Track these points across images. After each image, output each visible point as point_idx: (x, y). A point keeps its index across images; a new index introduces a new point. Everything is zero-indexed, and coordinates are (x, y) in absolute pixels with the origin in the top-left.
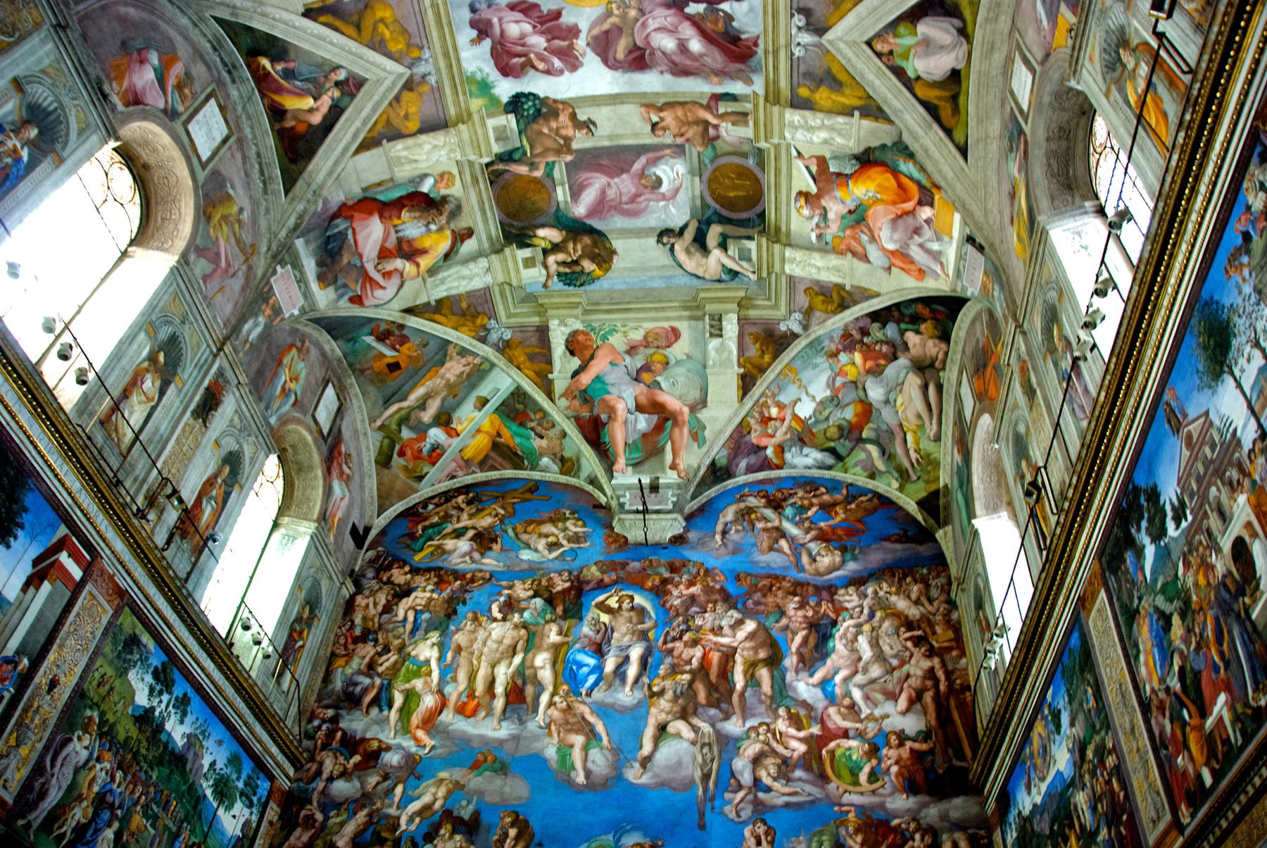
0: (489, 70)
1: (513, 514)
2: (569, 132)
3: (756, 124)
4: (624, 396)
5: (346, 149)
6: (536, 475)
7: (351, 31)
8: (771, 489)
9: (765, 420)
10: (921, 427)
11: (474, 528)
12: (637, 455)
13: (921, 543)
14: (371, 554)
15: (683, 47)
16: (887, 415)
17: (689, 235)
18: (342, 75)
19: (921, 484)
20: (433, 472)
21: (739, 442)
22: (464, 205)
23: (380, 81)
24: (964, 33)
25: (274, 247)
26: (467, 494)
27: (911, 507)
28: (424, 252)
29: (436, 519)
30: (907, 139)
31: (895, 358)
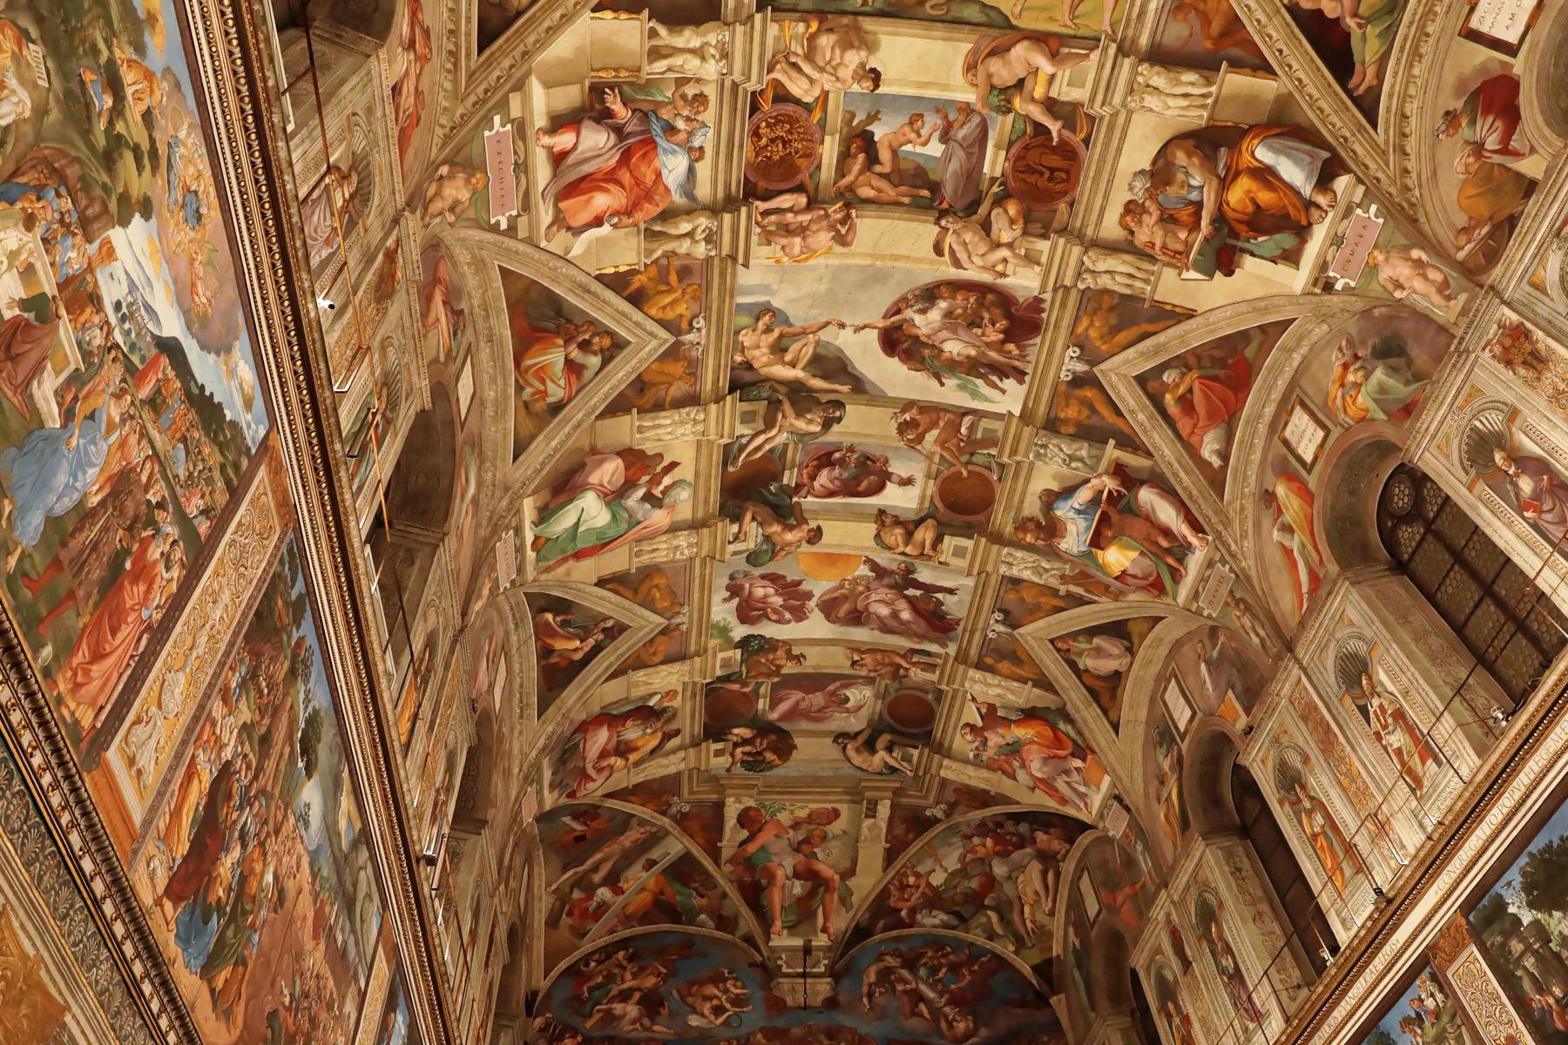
0: (732, 620)
1: (673, 973)
2: (783, 662)
3: (942, 674)
4: (785, 864)
5: (597, 679)
6: (692, 929)
7: (629, 594)
8: (903, 948)
9: (903, 887)
10: (1037, 902)
11: (639, 989)
12: (792, 918)
13: (1038, 1008)
14: (539, 1021)
15: (895, 614)
16: (1008, 888)
17: (861, 739)
18: (610, 623)
19: (1035, 951)
20: (595, 928)
21: (882, 909)
22: (679, 714)
23: (641, 628)
24: (1131, 651)
25: (525, 768)
26: (626, 949)
27: (1026, 970)
28: (636, 749)
29: (600, 979)
30: (1069, 707)
31: (1023, 847)
